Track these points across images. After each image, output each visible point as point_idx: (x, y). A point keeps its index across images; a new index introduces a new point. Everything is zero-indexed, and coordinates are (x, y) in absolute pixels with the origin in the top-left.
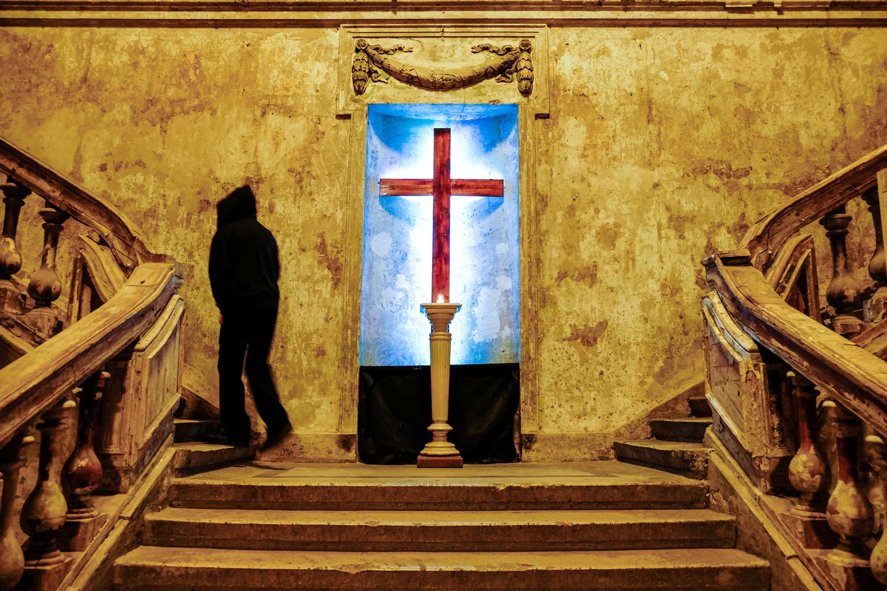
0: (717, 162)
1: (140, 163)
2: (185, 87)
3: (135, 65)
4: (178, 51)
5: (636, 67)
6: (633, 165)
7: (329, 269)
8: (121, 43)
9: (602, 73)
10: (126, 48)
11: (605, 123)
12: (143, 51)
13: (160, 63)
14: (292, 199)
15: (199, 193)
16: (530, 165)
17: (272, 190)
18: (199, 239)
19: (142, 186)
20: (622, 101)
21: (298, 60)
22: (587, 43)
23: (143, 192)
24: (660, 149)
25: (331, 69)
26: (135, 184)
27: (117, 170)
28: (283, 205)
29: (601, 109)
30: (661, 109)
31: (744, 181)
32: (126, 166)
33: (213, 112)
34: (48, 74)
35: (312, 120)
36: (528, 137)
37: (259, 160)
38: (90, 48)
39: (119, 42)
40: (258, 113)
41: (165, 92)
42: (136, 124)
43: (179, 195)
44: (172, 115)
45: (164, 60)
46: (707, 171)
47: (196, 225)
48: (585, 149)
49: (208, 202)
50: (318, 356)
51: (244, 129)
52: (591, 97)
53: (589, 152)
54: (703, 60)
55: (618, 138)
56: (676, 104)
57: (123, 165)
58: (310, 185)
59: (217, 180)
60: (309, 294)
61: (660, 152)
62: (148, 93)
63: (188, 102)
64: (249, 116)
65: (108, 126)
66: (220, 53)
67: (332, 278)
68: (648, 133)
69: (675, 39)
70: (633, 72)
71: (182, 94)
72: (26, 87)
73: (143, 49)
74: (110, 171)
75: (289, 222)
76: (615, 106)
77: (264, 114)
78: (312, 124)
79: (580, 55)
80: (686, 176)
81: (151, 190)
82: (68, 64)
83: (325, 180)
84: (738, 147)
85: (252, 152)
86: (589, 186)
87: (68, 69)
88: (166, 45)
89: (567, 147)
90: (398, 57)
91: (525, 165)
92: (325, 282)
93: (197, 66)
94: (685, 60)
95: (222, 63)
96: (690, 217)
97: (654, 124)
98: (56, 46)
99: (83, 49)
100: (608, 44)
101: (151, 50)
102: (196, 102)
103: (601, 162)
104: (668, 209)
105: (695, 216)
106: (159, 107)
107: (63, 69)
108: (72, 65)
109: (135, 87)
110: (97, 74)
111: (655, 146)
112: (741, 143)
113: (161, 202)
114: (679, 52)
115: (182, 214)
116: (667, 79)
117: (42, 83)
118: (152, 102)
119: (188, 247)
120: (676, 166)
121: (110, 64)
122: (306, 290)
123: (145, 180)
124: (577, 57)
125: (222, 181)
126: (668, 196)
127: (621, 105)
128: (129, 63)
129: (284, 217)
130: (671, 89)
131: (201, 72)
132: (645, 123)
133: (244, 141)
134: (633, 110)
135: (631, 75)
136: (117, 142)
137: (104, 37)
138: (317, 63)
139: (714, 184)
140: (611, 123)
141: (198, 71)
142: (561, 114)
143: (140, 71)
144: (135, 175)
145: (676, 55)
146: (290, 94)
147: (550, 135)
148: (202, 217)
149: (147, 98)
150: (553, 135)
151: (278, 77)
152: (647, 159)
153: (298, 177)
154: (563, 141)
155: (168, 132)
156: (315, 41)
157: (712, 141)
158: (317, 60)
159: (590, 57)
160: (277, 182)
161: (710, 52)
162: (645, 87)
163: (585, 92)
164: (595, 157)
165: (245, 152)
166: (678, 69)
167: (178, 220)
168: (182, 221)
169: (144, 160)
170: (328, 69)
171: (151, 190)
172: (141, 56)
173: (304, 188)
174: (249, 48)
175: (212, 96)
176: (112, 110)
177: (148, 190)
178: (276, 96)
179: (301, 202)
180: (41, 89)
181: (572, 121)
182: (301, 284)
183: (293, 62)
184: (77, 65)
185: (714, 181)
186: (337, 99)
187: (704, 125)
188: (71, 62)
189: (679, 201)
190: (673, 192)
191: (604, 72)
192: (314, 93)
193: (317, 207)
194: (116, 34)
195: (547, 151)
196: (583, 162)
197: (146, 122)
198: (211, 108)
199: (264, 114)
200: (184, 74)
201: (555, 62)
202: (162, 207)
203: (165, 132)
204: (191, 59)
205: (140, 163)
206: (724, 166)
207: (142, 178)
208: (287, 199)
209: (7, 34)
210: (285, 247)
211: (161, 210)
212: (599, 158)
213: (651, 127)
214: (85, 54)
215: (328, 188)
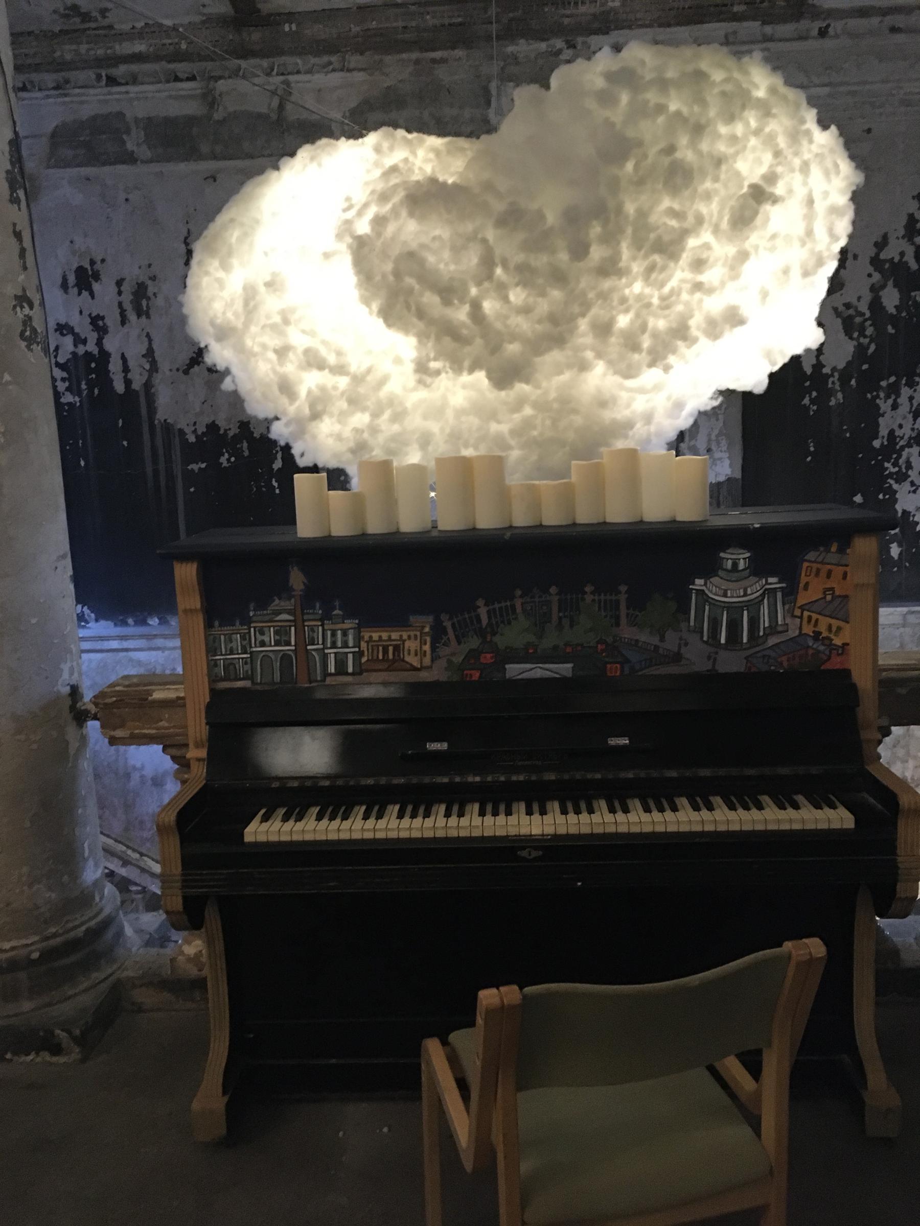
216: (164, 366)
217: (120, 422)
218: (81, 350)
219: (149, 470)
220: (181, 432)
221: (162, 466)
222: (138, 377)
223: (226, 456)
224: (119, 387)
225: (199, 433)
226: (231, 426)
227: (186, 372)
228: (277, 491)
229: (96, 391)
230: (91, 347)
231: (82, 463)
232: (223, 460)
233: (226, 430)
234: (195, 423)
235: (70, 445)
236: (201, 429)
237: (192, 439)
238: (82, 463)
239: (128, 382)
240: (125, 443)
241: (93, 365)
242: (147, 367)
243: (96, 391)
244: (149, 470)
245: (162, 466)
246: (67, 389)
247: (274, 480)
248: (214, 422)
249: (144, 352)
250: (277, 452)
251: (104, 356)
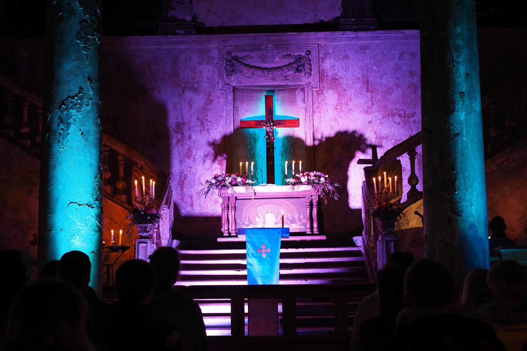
0: (399, 111)
5: (362, 64)
6: (359, 113)
7: (218, 164)
9: (345, 67)
11: (346, 93)
14: (199, 132)
16: (310, 114)
17: (190, 128)
20: (354, 82)
21: (198, 64)
22: (338, 53)
24: (372, 104)
25: (215, 68)
28: (195, 135)
29: (344, 86)
30: (373, 85)
31: (412, 119)
35: (207, 94)
36: (309, 100)
37: (183, 114)
40: (181, 91)
46: (394, 114)
48: (336, 105)
50: (215, 204)
52: (339, 80)
53: (339, 107)
54: (394, 60)
55: (353, 99)
56: (381, 82)
58: (208, 125)
60: (210, 176)
61: (372, 106)
67: (220, 169)
68: (366, 97)
69: (381, 49)
70: (360, 67)
75: (199, 143)
76: (351, 84)
78: (207, 96)
79: (334, 59)
80: (384, 117)
83: (215, 123)
84: (409, 103)
86: (338, 123)
89: (328, 104)
90: (247, 62)
91: (308, 114)
92: (217, 170)
94: (386, 60)
96: (386, 137)
97: (370, 93)
100: (348, 53)
103: (344, 111)
104: (375, 133)
105: (388, 136)
111: (370, 103)
112: (411, 101)
114: (383, 56)
116: (376, 70)
120: (380, 113)
122: (208, 174)
124: (333, 60)
126: (376, 127)
127: (354, 83)
129: (196, 141)
130: (378, 75)
132: (365, 92)
134: (359, 86)
135: (359, 69)
138: (207, 65)
139: (397, 121)
140: (349, 92)
142: (325, 88)
145: (381, 58)
146: (195, 81)
147: (320, 98)
150: (321, 99)
151: (189, 73)
152: (366, 109)
153: (201, 121)
154: (326, 102)
156: (206, 54)
157: (397, 100)
158: (207, 64)
159: (339, 60)
160: (192, 124)
161: (398, 56)
162: (366, 74)
163: (337, 77)
164: (341, 109)
166: (382, 64)
170: (213, 69)
173: (205, 127)
178: (189, 83)
179: (204, 134)
181: (331, 92)
182: (206, 171)
183: (196, 65)
185: (397, 119)
186: (218, 84)
187: (394, 93)
189: (381, 130)
190: (378, 125)
191: (346, 67)
192: (207, 81)
193: (211, 136)
195: (318, 107)
196: (336, 111)
199: (183, 91)
201: (322, 63)
206: (403, 112)
208: (197, 132)
210: (198, 155)
212: (343, 109)
213: (368, 94)
215: (216, 127)
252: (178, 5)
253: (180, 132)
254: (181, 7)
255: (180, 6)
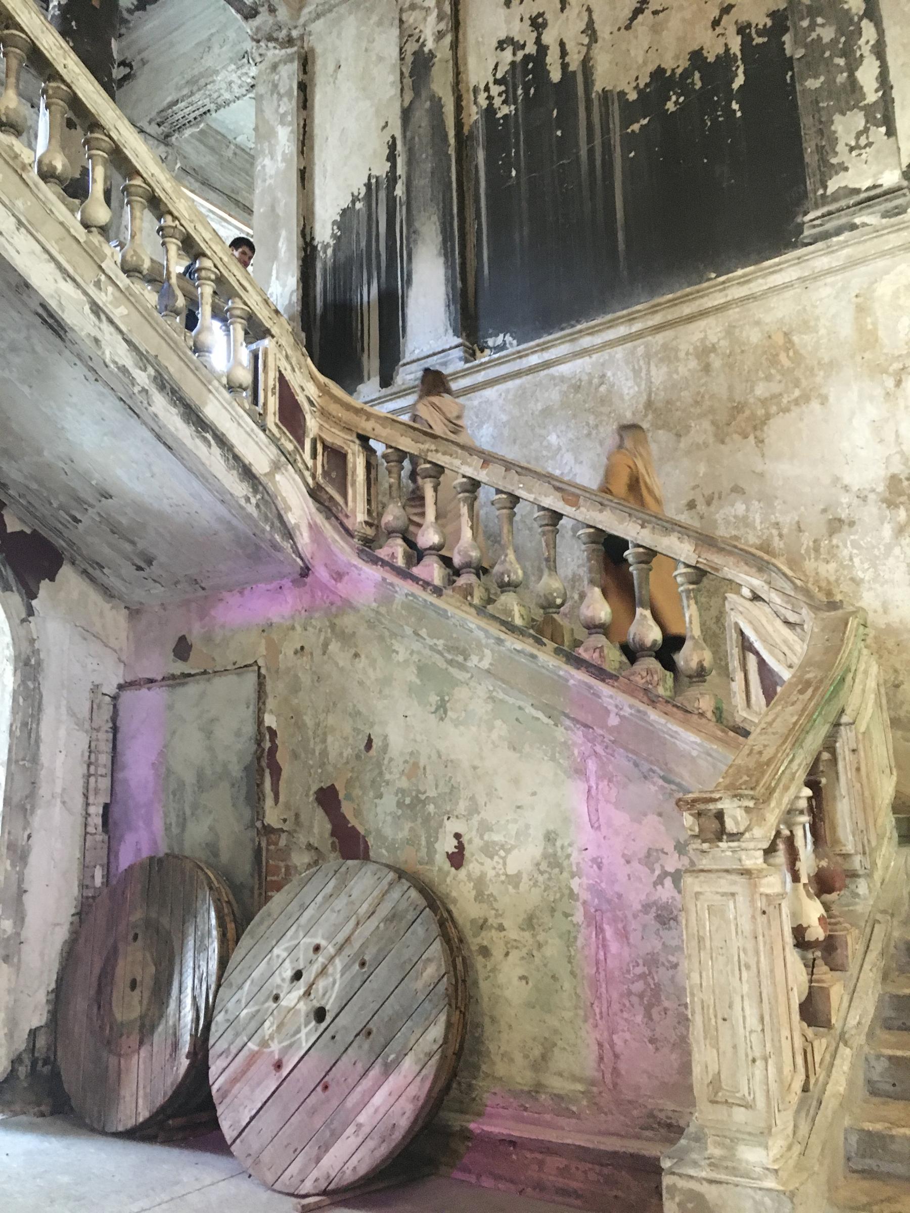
1: (737, 490)
2: (778, 377)
3: (707, 368)
4: (760, 335)
8: (684, 347)
10: (691, 351)
12: (714, 349)
13: (738, 357)
15: (824, 511)
18: (837, 571)
19: (745, 518)
23: (747, 525)
26: (735, 517)
27: (709, 503)
32: (720, 498)
33: (824, 400)
34: (605, 410)
38: (649, 363)
39: (682, 347)
40: (890, 383)
41: (752, 390)
42: (723, 442)
43: (797, 518)
44: (768, 417)
45: (743, 352)
47: (829, 553)
49: (840, 520)
51: (872, 411)
57: (716, 496)
59: (846, 488)
62: (730, 399)
63: (785, 396)
64: (879, 392)
65: (688, 453)
66: (817, 319)
71: (775, 388)
72: (585, 432)
73: (713, 345)
74: (701, 507)
77: (898, 383)
81: (758, 521)
82: (626, 391)
85: (892, 438)
87: (627, 398)
88: (741, 332)
93: (789, 344)
95: (823, 331)
98: (609, 374)
99: (641, 369)
101: (723, 343)
102: (797, 393)
106: (747, 413)
107: (622, 399)
108: (632, 391)
109: (712, 397)
110: (662, 393)
113: (775, 532)
115: (805, 543)
117: (601, 422)
118: (738, 409)
119: (824, 584)
121: (675, 376)
123: (747, 510)
125: (855, 488)
128: (699, 368)
131: (796, 352)
133: (877, 427)
136: (702, 469)
137: (662, 346)
141: (791, 353)
143: (714, 374)
144: (733, 506)
148: (835, 541)
149: (729, 405)
155: (766, 441)
165: (881, 441)
167: (803, 552)
168: (807, 550)
169: (742, 484)
171: (758, 521)
172: (712, 355)
174: (859, 300)
175: (818, 379)
176: (689, 432)
177: (754, 521)
180: (601, 429)
184: (636, 389)
188: (630, 388)
194: (676, 338)
197: (736, 436)
198: (820, 395)
199: (898, 383)
200: (774, 361)
202: (777, 539)
203: (762, 441)
204: (779, 340)
205: (737, 490)
207: (744, 507)
209: (553, 378)
211: (777, 543)
214: (643, 374)
216: (604, 30)
217: (555, 112)
218: (520, 54)
219: (583, 153)
220: (622, 94)
221: (598, 142)
222: (576, 57)
223: (674, 98)
224: (556, 75)
225: (642, 86)
226: (680, 62)
227: (628, 27)
228: (739, 114)
229: (532, 91)
230: (531, 49)
231: (514, 173)
232: (670, 106)
233: (673, 70)
234: (637, 78)
235: (502, 159)
236: (644, 80)
237: (633, 96)
238: (514, 173)
239: (565, 66)
240: (559, 133)
241: (531, 65)
242: (586, 41)
243: (532, 91)
244: (583, 153)
245: (598, 142)
246: (504, 102)
247: (734, 102)
248: (659, 66)
249: (583, 27)
250: (738, 67)
251: (542, 49)
252: (854, 153)
253: (902, 503)
254: (864, 156)
255: (860, 155)
